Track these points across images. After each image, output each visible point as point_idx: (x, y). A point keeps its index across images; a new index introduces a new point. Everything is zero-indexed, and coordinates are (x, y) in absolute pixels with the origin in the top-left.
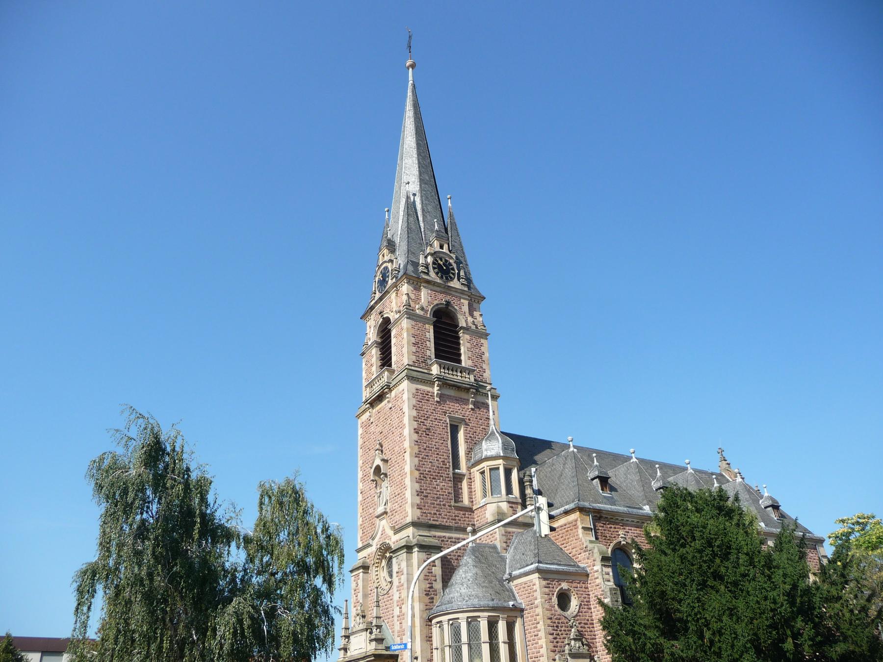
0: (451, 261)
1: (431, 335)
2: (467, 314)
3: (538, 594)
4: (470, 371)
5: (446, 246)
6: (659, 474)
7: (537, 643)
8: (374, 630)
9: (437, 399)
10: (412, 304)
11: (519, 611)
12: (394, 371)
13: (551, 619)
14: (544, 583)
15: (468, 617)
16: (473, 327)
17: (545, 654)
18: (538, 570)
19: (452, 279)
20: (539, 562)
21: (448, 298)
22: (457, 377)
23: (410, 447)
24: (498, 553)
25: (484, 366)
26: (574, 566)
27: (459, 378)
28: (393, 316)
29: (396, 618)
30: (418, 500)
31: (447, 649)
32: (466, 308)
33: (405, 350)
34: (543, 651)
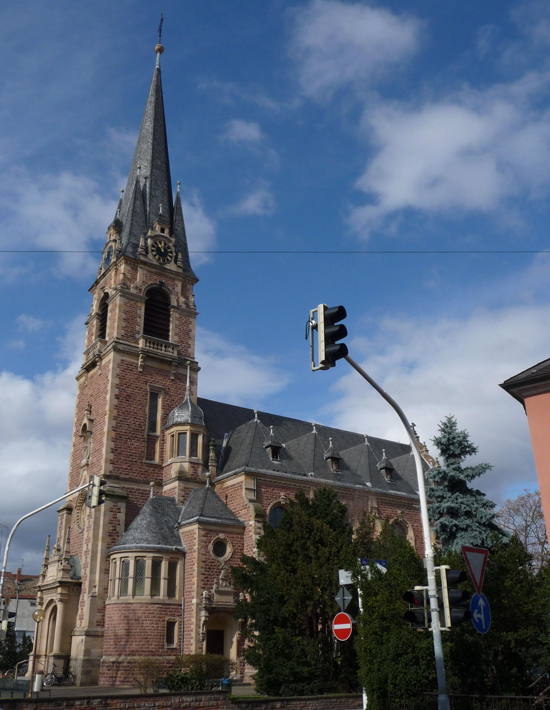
0: (171, 245)
1: (142, 312)
2: (180, 295)
3: (196, 541)
4: (174, 346)
6: (331, 445)
8: (63, 562)
9: (140, 370)
10: (128, 283)
11: (183, 554)
12: (106, 342)
13: (205, 562)
14: (203, 533)
15: (136, 557)
16: (184, 306)
17: (195, 591)
18: (198, 522)
19: (169, 262)
22: (162, 351)
23: (110, 410)
24: (175, 505)
28: (111, 292)
29: (83, 553)
30: (111, 456)
31: (117, 581)
32: (179, 289)
33: (116, 324)
34: (195, 587)
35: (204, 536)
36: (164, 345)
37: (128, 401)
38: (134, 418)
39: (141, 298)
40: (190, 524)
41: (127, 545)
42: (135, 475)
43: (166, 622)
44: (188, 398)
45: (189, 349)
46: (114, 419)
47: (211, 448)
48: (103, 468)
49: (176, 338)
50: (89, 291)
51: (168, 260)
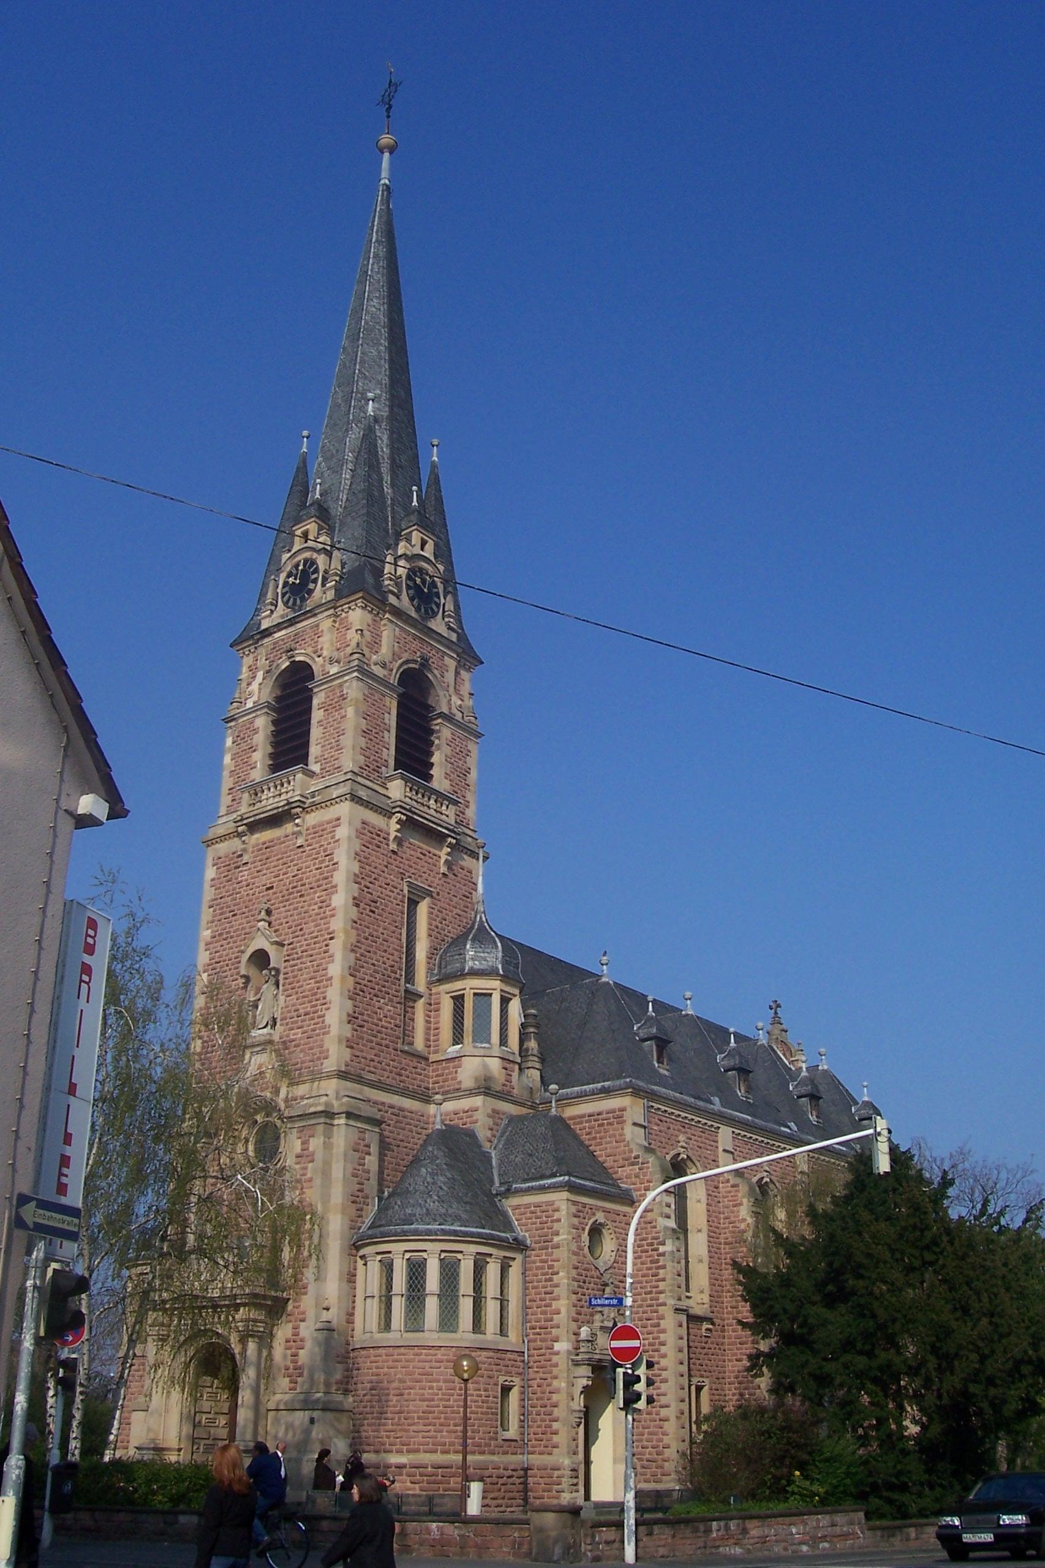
1: (392, 720)
2: (451, 689)
5: (430, 546)
7: (550, 1305)
9: (393, 846)
12: (311, 774)
19: (435, 614)
23: (346, 932)
26: (613, 1185)
32: (450, 677)
34: (562, 1318)
37: (374, 912)
38: (385, 951)
40: (543, 1189)
42: (386, 1074)
45: (467, 811)
46: (352, 950)
47: (532, 1030)
48: (335, 1056)
51: (432, 609)
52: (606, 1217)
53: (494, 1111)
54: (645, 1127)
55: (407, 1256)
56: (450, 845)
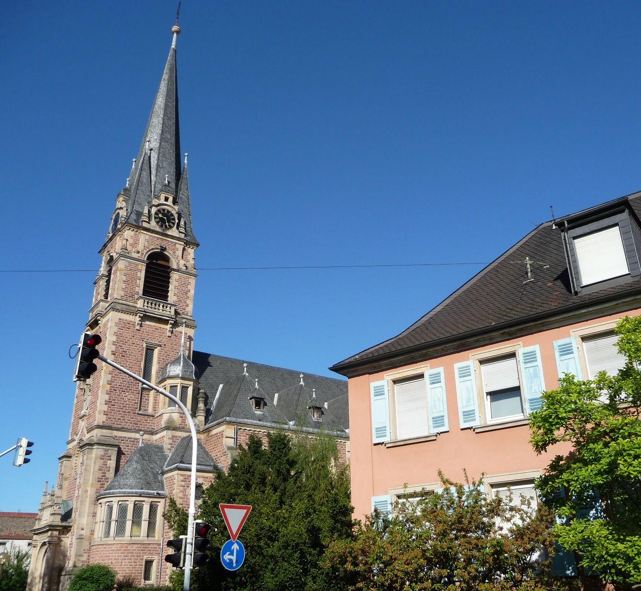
0: (174, 212)
1: (142, 275)
2: (180, 258)
6: (314, 396)
9: (138, 327)
10: (129, 248)
19: (171, 227)
20: (182, 462)
21: (164, 244)
25: (188, 302)
27: (161, 311)
28: (115, 256)
29: (75, 498)
32: (180, 253)
35: (182, 481)
36: (161, 305)
37: (124, 356)
39: (143, 261)
40: (171, 471)
41: (112, 491)
43: (144, 561)
44: (182, 354)
45: (187, 308)
49: (175, 298)
50: (99, 252)
52: (204, 480)
53: (173, 436)
54: (234, 438)
55: (107, 504)
56: (171, 324)
